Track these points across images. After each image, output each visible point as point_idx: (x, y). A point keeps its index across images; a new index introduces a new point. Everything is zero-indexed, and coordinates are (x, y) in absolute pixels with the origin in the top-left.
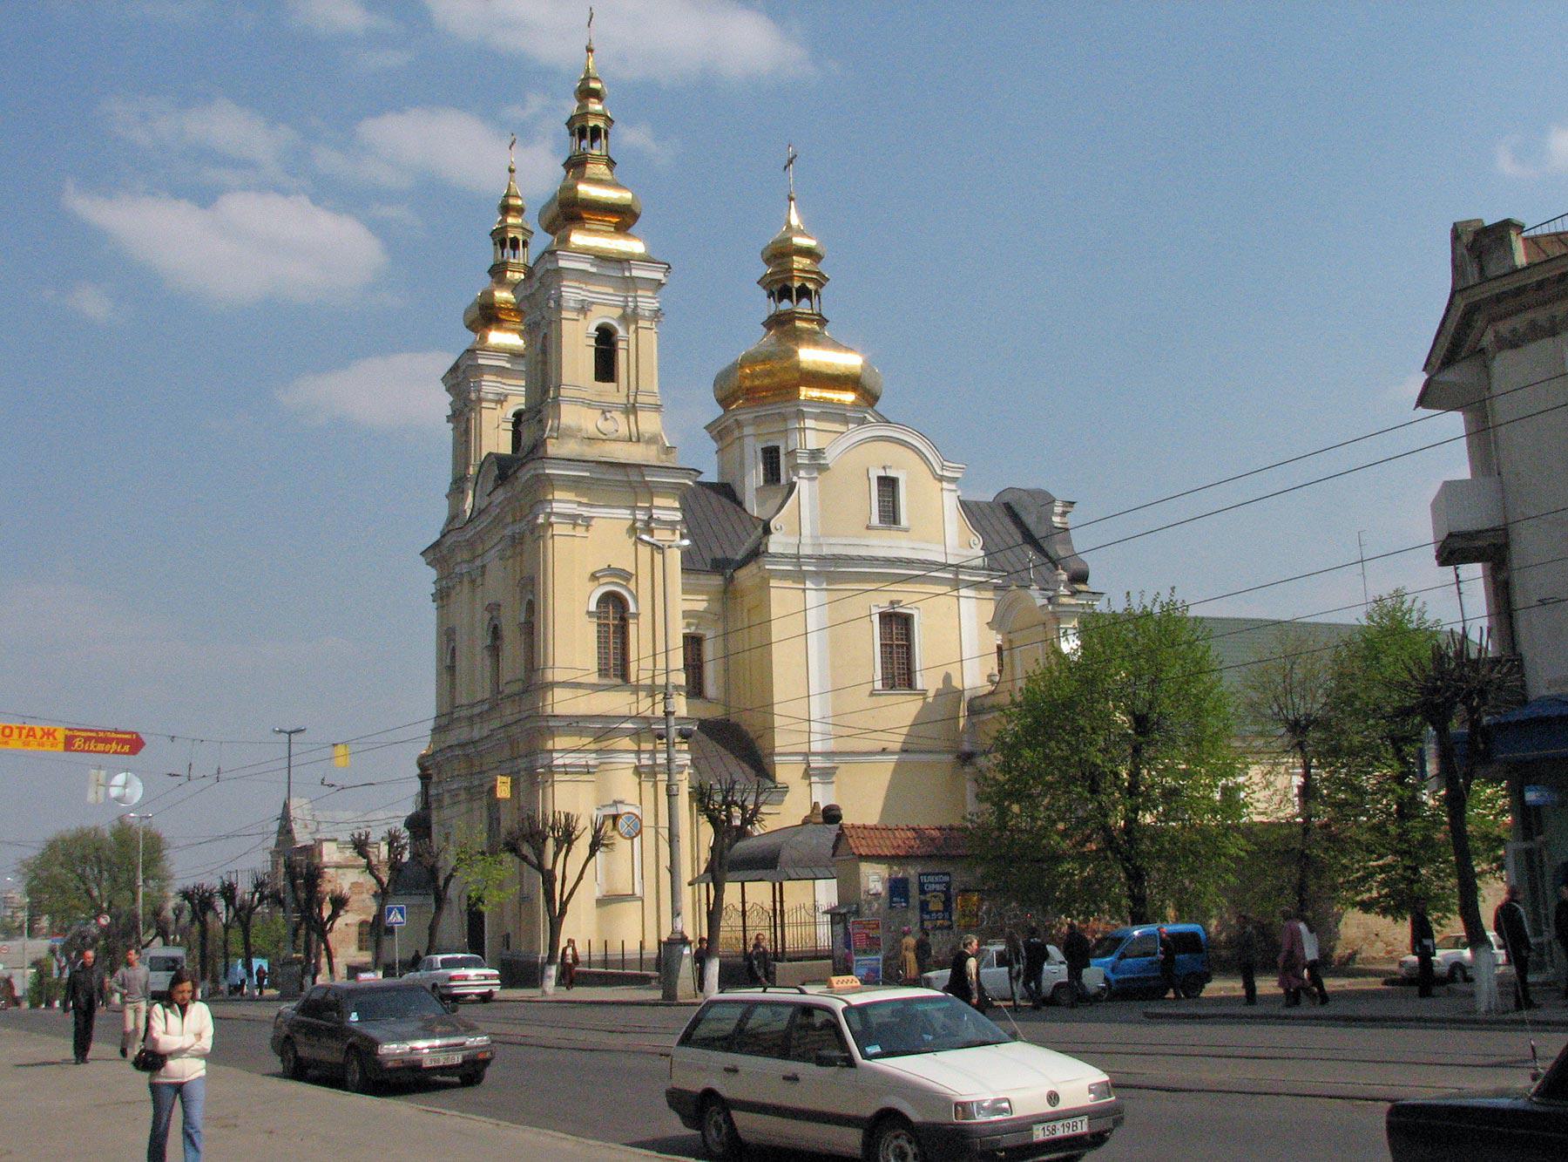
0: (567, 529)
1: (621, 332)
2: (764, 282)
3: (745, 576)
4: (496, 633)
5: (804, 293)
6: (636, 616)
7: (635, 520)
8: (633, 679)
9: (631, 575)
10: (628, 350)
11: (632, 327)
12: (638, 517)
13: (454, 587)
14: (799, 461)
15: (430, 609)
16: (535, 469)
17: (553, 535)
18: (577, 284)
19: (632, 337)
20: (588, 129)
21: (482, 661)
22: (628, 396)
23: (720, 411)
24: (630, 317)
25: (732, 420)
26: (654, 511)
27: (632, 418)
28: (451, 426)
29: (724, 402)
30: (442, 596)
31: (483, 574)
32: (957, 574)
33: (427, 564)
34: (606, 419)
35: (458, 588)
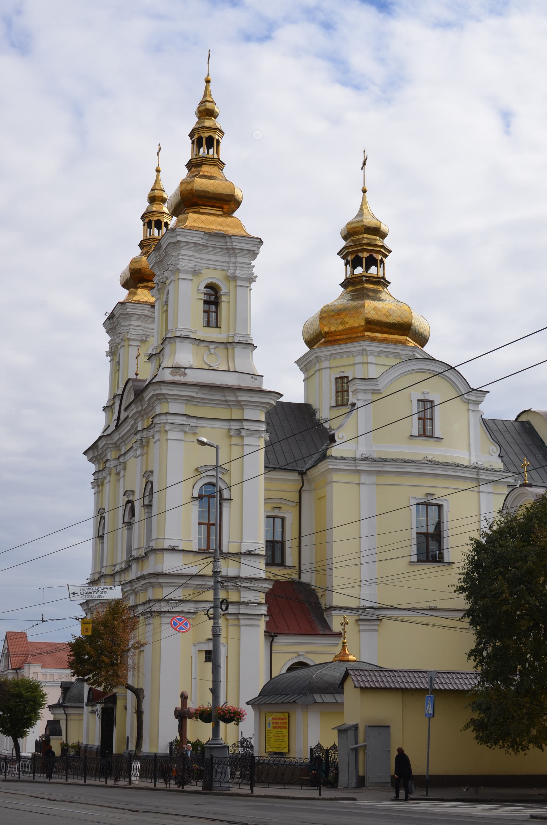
1: (224, 289)
2: (343, 254)
5: (371, 262)
10: (229, 302)
13: (105, 478)
15: (90, 494)
16: (154, 390)
18: (190, 253)
20: (204, 139)
21: (122, 534)
23: (308, 349)
25: (314, 357)
28: (109, 358)
29: (310, 343)
31: (125, 468)
33: (89, 460)
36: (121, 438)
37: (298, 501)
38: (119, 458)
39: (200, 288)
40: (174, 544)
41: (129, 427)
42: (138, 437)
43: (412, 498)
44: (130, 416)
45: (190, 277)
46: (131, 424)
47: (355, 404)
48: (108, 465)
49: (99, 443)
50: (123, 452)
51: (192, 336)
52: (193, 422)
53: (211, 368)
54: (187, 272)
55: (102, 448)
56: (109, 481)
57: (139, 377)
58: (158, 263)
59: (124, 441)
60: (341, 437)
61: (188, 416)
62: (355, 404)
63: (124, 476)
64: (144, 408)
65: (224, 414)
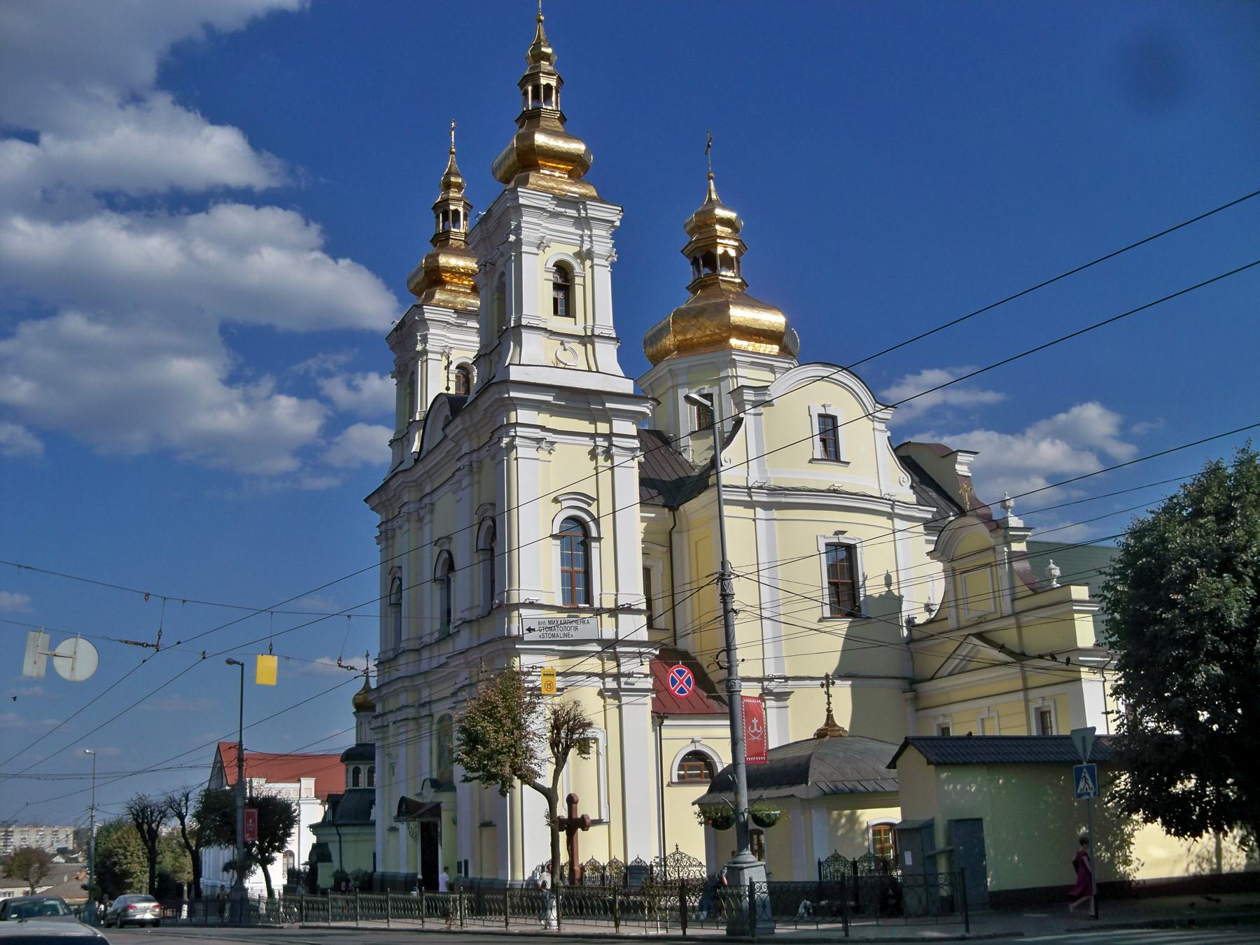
0: (532, 452)
1: (577, 269)
3: (694, 508)
4: (451, 567)
6: (599, 539)
7: (596, 446)
8: (597, 605)
9: (593, 499)
10: (584, 286)
11: (588, 263)
12: (598, 443)
13: (400, 528)
14: (745, 398)
17: (516, 459)
18: (535, 220)
19: (588, 271)
21: (431, 598)
22: (585, 328)
24: (585, 256)
26: (614, 439)
27: (589, 347)
30: (386, 535)
31: (432, 512)
32: (892, 509)
33: (372, 509)
34: (565, 350)
35: (406, 527)
36: (427, 472)
37: (668, 545)
38: (421, 499)
39: (547, 266)
40: (533, 597)
41: (443, 455)
42: (465, 461)
43: (821, 536)
44: (450, 437)
45: (535, 250)
46: (446, 451)
47: (743, 418)
48: (404, 510)
49: (392, 483)
50: (428, 490)
51: (542, 325)
52: (550, 437)
53: (567, 367)
54: (530, 244)
55: (395, 489)
56: (409, 530)
57: (450, 392)
58: (484, 239)
59: (430, 477)
60: (728, 460)
61: (543, 428)
62: (743, 418)
63: (431, 521)
64: (475, 421)
65: (586, 427)
